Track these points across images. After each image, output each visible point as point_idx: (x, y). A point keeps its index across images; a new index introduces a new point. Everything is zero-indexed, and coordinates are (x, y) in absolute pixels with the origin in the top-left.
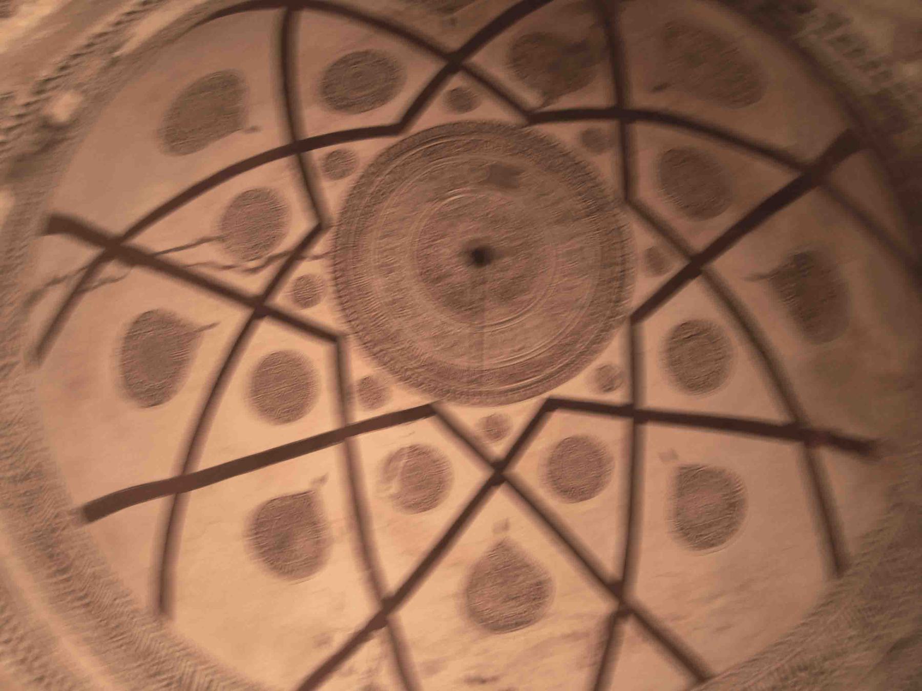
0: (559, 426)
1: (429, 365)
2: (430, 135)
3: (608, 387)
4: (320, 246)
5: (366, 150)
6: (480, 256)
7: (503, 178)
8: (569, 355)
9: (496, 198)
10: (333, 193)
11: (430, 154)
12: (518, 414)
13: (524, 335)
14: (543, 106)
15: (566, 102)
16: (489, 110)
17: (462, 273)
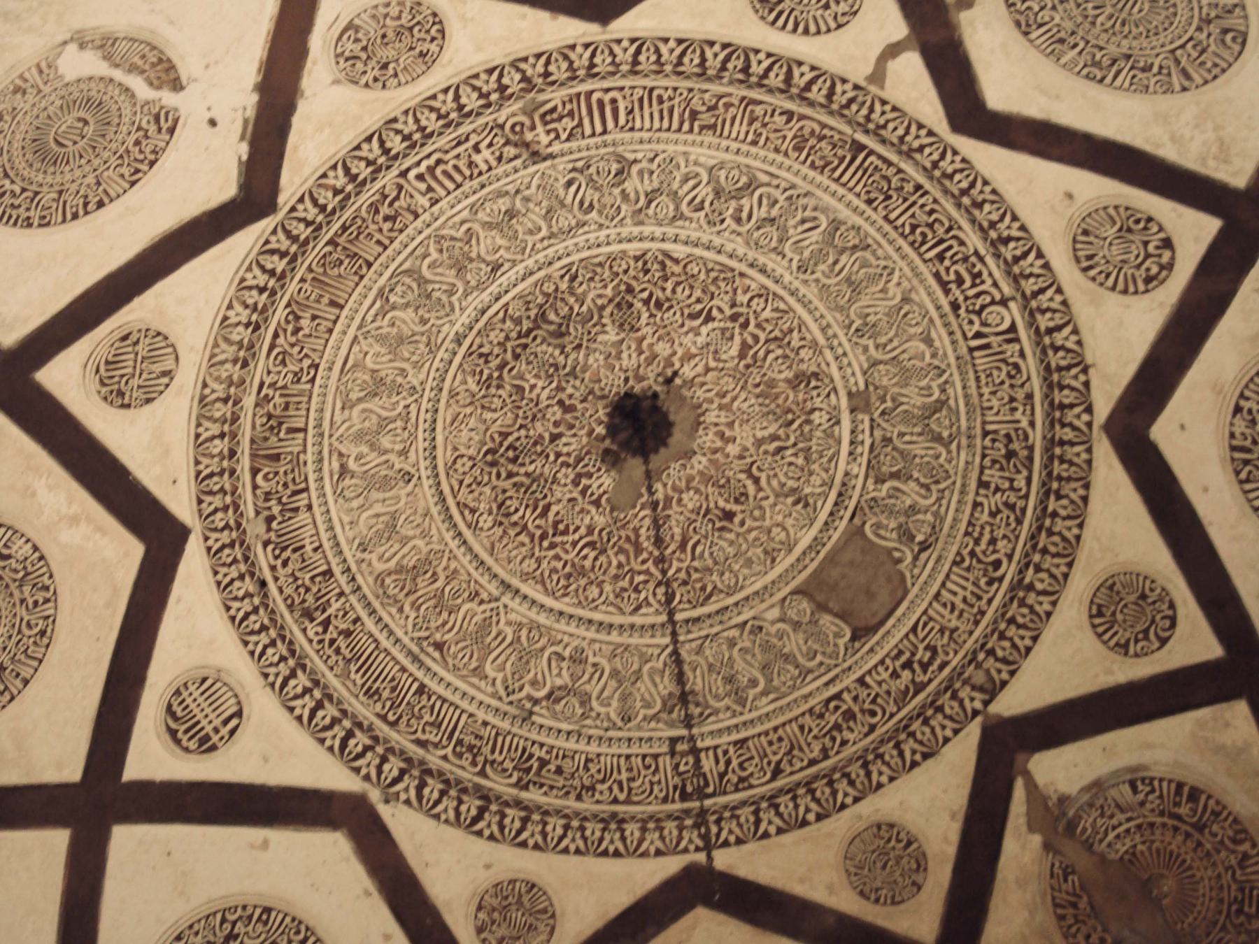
0: (94, 557)
1: (392, 214)
2: (1065, 488)
3: (185, 731)
4: (913, 87)
5: (1119, 332)
6: (640, 425)
7: (849, 590)
8: (292, 614)
9: (805, 537)
10: (1046, 196)
11: (1012, 454)
12: (155, 444)
13: (385, 490)
14: (1031, 785)
15: (1020, 850)
16: (1064, 661)
17: (614, 362)
